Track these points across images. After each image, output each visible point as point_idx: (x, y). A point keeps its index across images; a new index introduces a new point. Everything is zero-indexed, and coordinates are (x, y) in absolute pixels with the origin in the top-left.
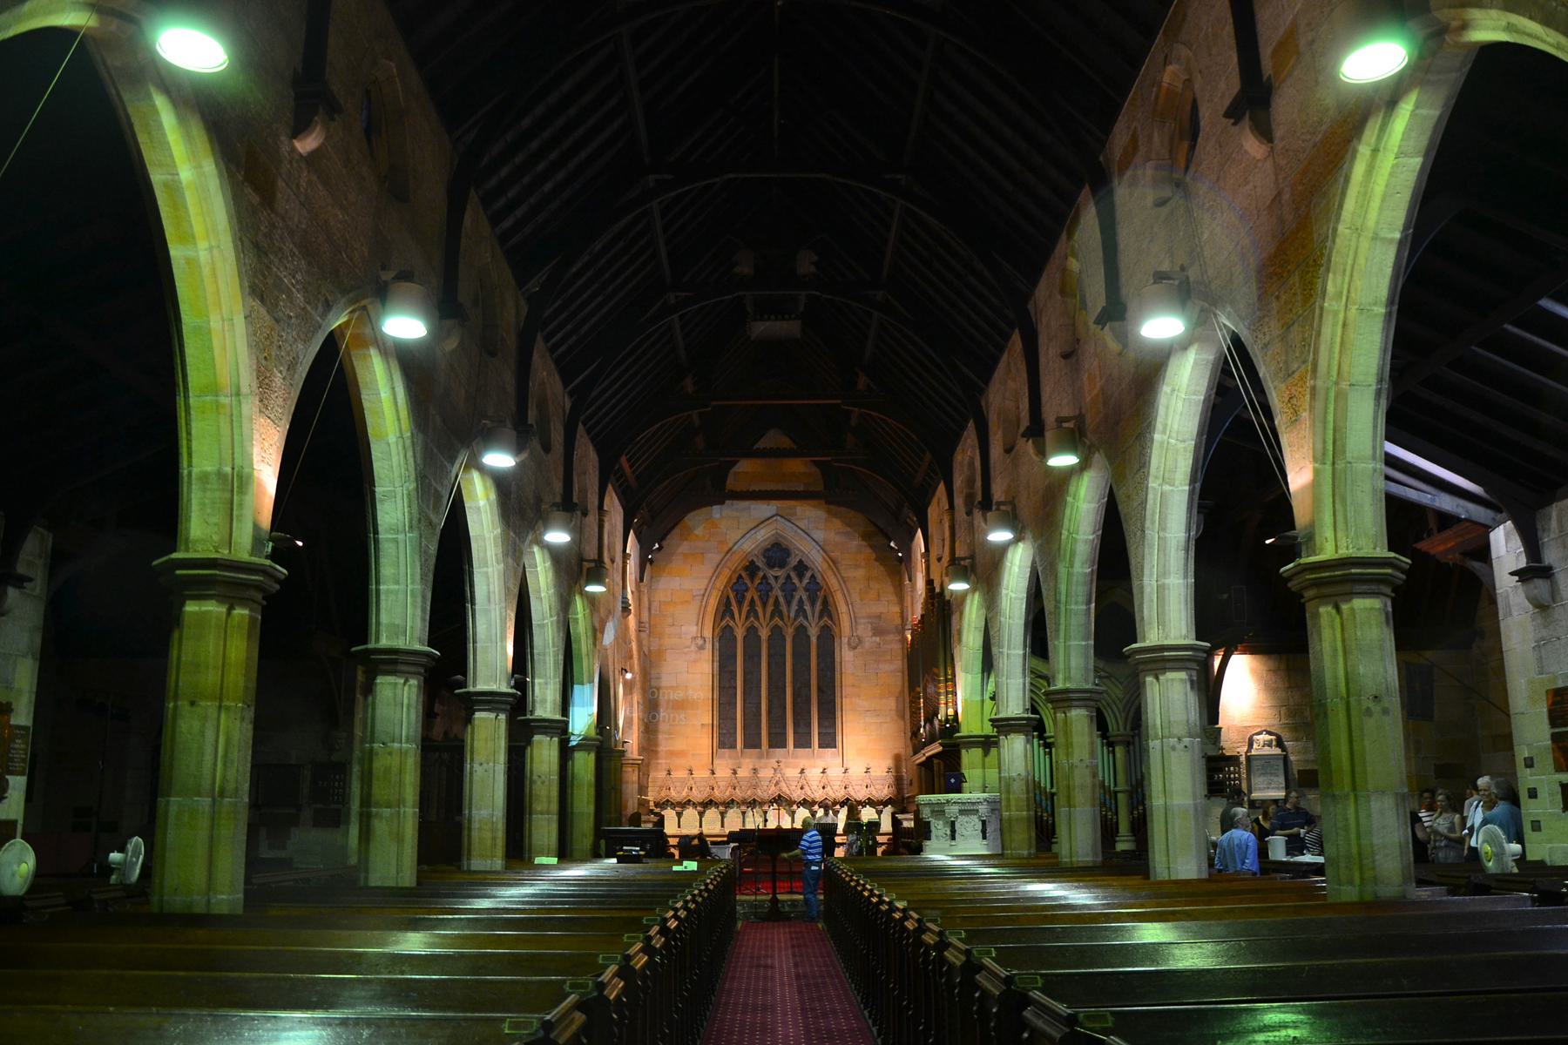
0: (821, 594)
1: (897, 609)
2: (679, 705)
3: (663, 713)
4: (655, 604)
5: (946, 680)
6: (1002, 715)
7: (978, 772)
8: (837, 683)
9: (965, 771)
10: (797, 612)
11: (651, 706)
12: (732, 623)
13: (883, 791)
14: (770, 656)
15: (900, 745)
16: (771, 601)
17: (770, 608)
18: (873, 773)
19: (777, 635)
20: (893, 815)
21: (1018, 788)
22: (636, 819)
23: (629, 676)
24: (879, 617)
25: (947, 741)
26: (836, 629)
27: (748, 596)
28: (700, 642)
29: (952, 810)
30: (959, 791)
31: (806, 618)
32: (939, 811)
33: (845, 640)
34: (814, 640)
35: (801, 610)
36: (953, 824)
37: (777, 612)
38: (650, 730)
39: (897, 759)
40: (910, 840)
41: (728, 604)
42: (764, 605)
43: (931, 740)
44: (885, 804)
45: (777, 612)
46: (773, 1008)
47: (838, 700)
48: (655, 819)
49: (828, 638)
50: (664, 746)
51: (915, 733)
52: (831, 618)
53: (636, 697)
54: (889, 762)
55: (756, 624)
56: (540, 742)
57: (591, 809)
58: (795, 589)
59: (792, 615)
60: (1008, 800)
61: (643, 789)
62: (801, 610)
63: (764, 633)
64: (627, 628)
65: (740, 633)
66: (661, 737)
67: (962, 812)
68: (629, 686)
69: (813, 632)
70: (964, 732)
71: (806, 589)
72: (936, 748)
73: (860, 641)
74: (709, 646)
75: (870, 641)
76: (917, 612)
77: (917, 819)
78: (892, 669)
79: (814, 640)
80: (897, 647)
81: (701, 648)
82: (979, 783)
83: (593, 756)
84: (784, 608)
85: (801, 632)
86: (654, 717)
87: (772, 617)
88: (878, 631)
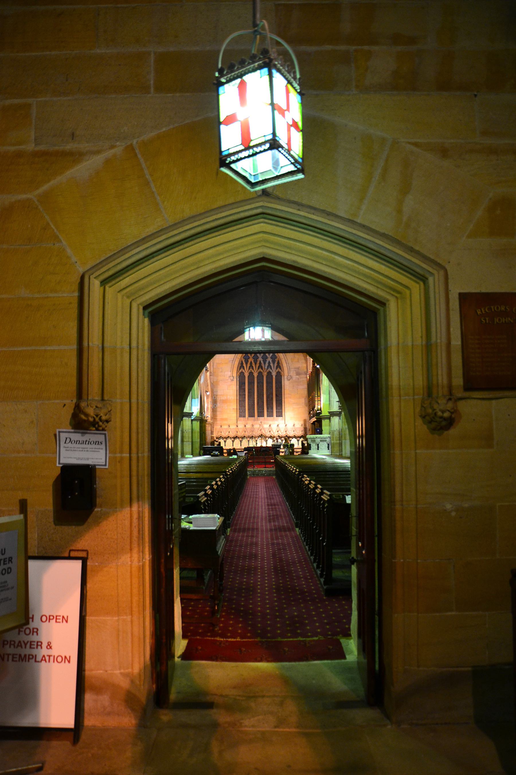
0: (277, 360)
1: (305, 365)
2: (225, 402)
3: (218, 405)
4: (215, 364)
5: (318, 396)
6: (332, 411)
7: (328, 428)
8: (283, 393)
9: (323, 428)
10: (268, 367)
11: (214, 402)
12: (243, 371)
13: (300, 433)
14: (258, 383)
15: (306, 416)
16: (258, 362)
17: (258, 365)
18: (296, 426)
19: (260, 375)
20: (302, 441)
21: (336, 434)
22: (213, 443)
23: (208, 393)
24: (298, 368)
25: (318, 417)
26: (282, 373)
27: (250, 360)
28: (232, 378)
29: (318, 440)
30: (321, 433)
31: (271, 369)
32: (314, 441)
33: (286, 377)
34: (274, 377)
35: (269, 366)
36: (318, 445)
37: (260, 366)
38: (214, 410)
39: (305, 421)
40: (306, 449)
41: (242, 363)
42: (256, 364)
43: (313, 417)
44: (300, 437)
45: (260, 366)
46: (259, 492)
47: (283, 399)
48: (217, 443)
49: (279, 376)
50: (219, 416)
51: (310, 413)
52: (280, 369)
53: (210, 400)
54: (302, 422)
55: (253, 371)
56: (185, 420)
57: (199, 440)
58: (267, 358)
59: (266, 368)
60: (333, 437)
61: (212, 433)
62: (269, 366)
63: (256, 375)
64: (207, 376)
65: (247, 375)
66: (218, 413)
67: (321, 441)
68: (208, 396)
69: (274, 374)
70: (323, 414)
71: (271, 358)
72: (314, 419)
73: (291, 377)
74: (235, 380)
75: (295, 377)
76: (310, 370)
77: (308, 443)
78: (303, 389)
79: (274, 377)
80: (306, 379)
81: (232, 380)
82: (328, 431)
83: (199, 422)
84: (263, 365)
85: (269, 374)
86: (215, 406)
87: (258, 369)
88: (298, 374)
